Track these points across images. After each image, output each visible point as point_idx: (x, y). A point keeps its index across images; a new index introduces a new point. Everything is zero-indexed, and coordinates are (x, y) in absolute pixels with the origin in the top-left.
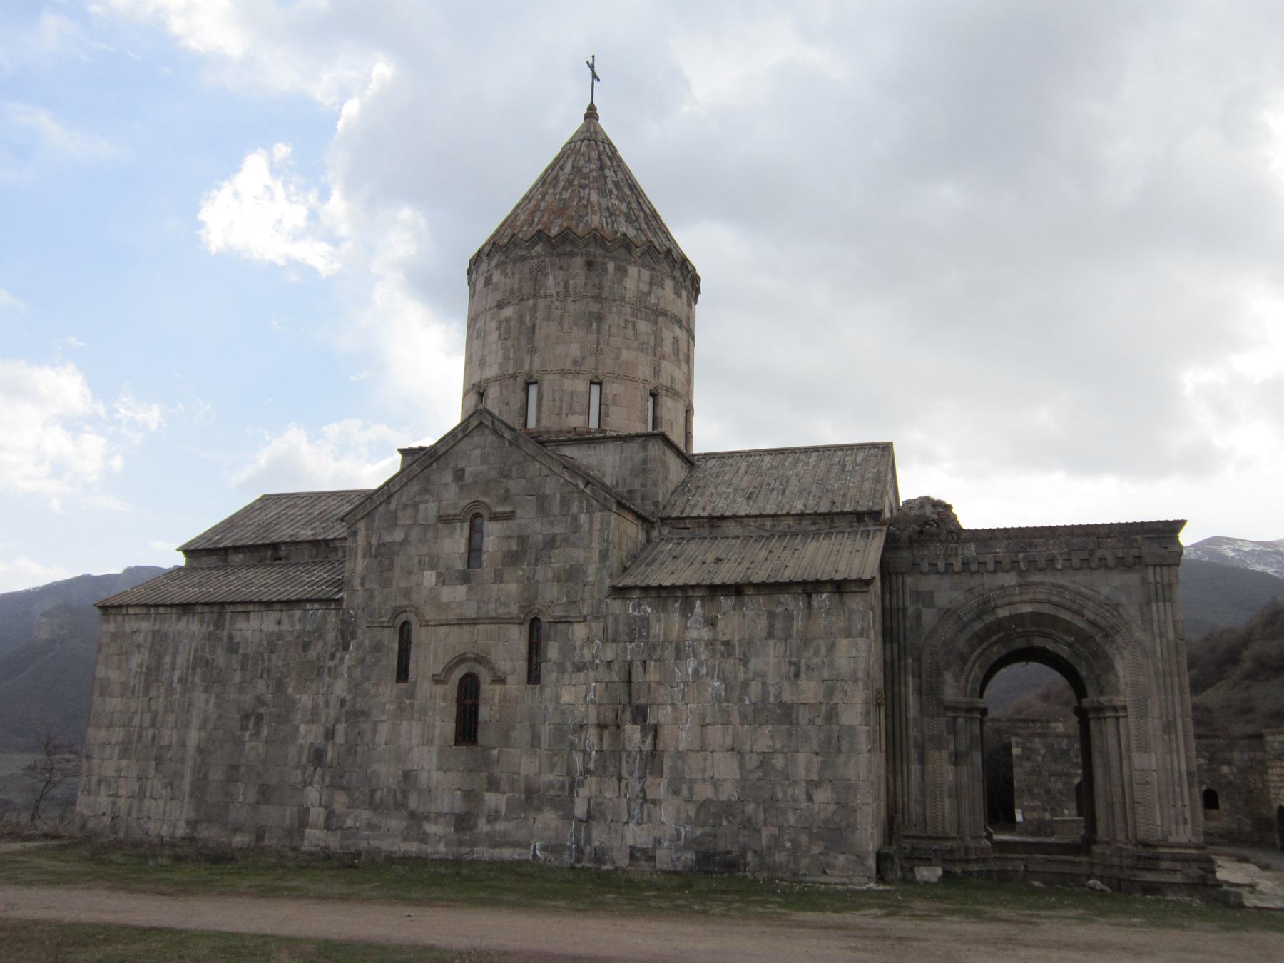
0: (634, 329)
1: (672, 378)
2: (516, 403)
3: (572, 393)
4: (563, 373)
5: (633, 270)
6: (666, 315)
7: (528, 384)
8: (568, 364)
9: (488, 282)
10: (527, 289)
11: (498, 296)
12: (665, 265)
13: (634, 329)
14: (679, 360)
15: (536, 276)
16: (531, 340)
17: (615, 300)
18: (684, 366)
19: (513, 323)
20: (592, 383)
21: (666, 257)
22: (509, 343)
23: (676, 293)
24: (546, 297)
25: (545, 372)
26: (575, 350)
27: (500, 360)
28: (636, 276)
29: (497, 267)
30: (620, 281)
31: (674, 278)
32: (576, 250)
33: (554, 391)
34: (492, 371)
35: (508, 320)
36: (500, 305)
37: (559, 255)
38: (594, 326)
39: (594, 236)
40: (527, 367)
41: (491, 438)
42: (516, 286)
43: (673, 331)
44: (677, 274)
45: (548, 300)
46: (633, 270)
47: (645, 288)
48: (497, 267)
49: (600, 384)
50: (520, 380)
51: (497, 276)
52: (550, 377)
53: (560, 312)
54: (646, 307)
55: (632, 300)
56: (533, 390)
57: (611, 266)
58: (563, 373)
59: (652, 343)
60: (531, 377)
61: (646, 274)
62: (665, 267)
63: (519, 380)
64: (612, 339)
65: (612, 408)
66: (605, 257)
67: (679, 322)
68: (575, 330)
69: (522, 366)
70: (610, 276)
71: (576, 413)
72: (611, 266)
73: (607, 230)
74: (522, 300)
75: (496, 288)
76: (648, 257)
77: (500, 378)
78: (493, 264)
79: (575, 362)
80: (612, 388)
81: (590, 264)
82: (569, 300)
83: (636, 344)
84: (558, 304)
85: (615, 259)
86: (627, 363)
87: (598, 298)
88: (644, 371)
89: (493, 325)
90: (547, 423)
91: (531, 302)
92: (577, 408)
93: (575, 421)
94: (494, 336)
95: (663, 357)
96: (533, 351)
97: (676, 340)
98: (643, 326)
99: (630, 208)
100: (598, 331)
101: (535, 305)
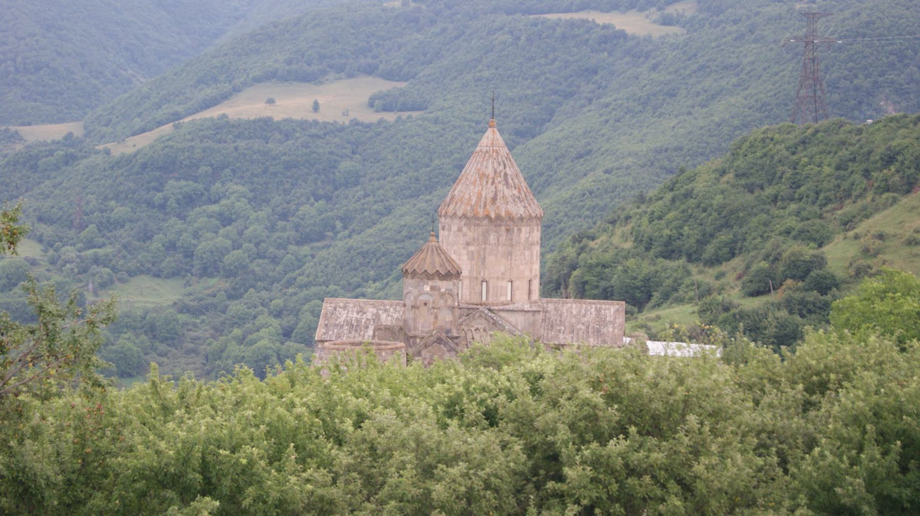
2: (477, 290)
4: (498, 278)
5: (523, 229)
8: (499, 275)
9: (460, 230)
10: (481, 238)
15: (485, 235)
16: (483, 263)
19: (476, 255)
22: (474, 262)
26: (502, 269)
35: (473, 252)
36: (468, 244)
41: (484, 321)
48: (465, 225)
50: (481, 279)
51: (465, 229)
56: (484, 284)
57: (516, 229)
58: (498, 278)
72: (516, 229)
73: (514, 212)
75: (465, 235)
78: (463, 223)
80: (516, 283)
81: (508, 230)
87: (511, 245)
88: (527, 273)
89: (464, 252)
90: (491, 300)
93: (502, 299)
94: (465, 257)
98: (527, 253)
99: (519, 192)
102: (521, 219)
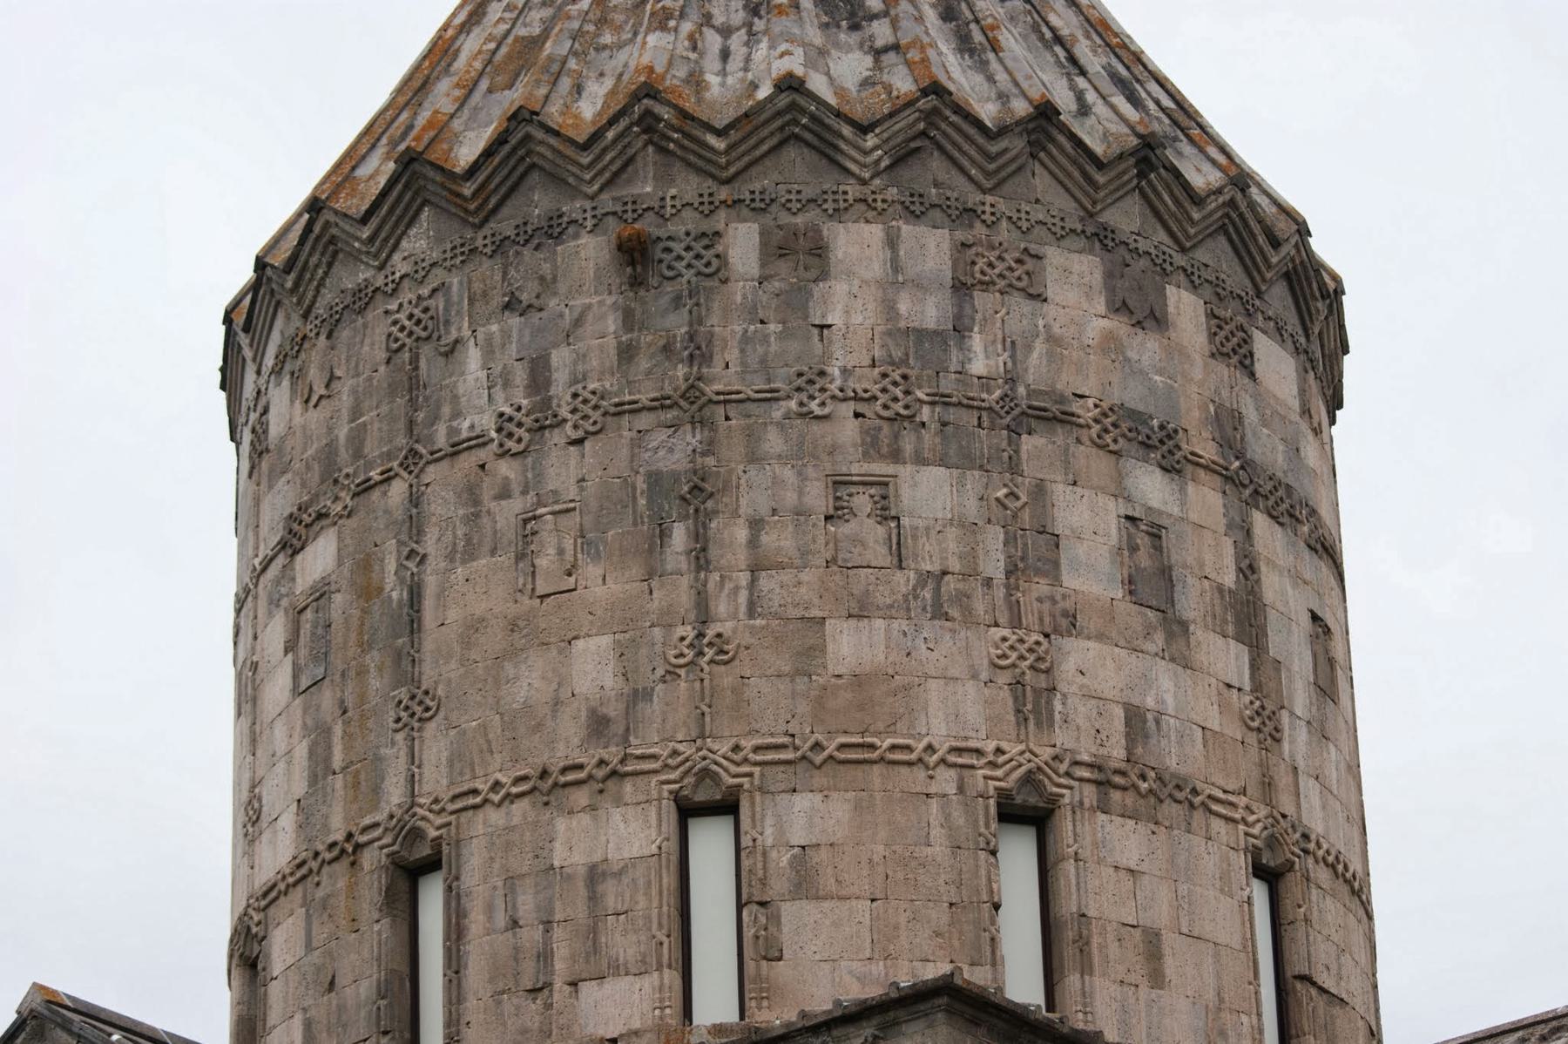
0: (885, 513)
1: (1137, 722)
3: (595, 875)
4: (547, 787)
5: (856, 244)
6: (1066, 419)
7: (410, 871)
8: (567, 743)
11: (281, 500)
12: (1041, 182)
13: (885, 513)
14: (1176, 628)
16: (405, 664)
17: (771, 397)
18: (1226, 658)
20: (688, 811)
21: (1036, 148)
22: (327, 698)
23: (1119, 307)
24: (457, 450)
25: (469, 801)
26: (593, 667)
27: (300, 787)
28: (875, 266)
29: (277, 371)
30: (795, 302)
31: (1102, 239)
32: (573, 208)
33: (511, 882)
34: (279, 851)
35: (321, 593)
37: (500, 247)
38: (679, 536)
39: (648, 123)
40: (394, 795)
42: (342, 433)
43: (1120, 492)
44: (1126, 217)
45: (468, 461)
46: (856, 244)
47: (931, 312)
49: (728, 807)
51: (283, 408)
52: (495, 817)
53: (516, 505)
54: (940, 400)
55: (866, 381)
57: (743, 244)
58: (547, 787)
59: (994, 564)
60: (416, 834)
61: (931, 248)
62: (1045, 192)
63: (369, 859)
64: (767, 582)
65: (788, 911)
66: (709, 208)
67: (1161, 445)
68: (592, 571)
69: (376, 790)
70: (739, 291)
71: (617, 969)
72: (743, 244)
74: (366, 488)
76: (936, 165)
77: (302, 873)
78: (269, 361)
79: (598, 725)
81: (635, 255)
82: (557, 437)
83: (903, 581)
84: (506, 469)
85: (759, 206)
86: (859, 680)
87: (692, 405)
91: (398, 489)
92: (623, 943)
95: (1068, 622)
96: (418, 710)
97: (1146, 531)
98: (929, 492)
100: (700, 557)
101: (415, 500)
102: (794, 119)
